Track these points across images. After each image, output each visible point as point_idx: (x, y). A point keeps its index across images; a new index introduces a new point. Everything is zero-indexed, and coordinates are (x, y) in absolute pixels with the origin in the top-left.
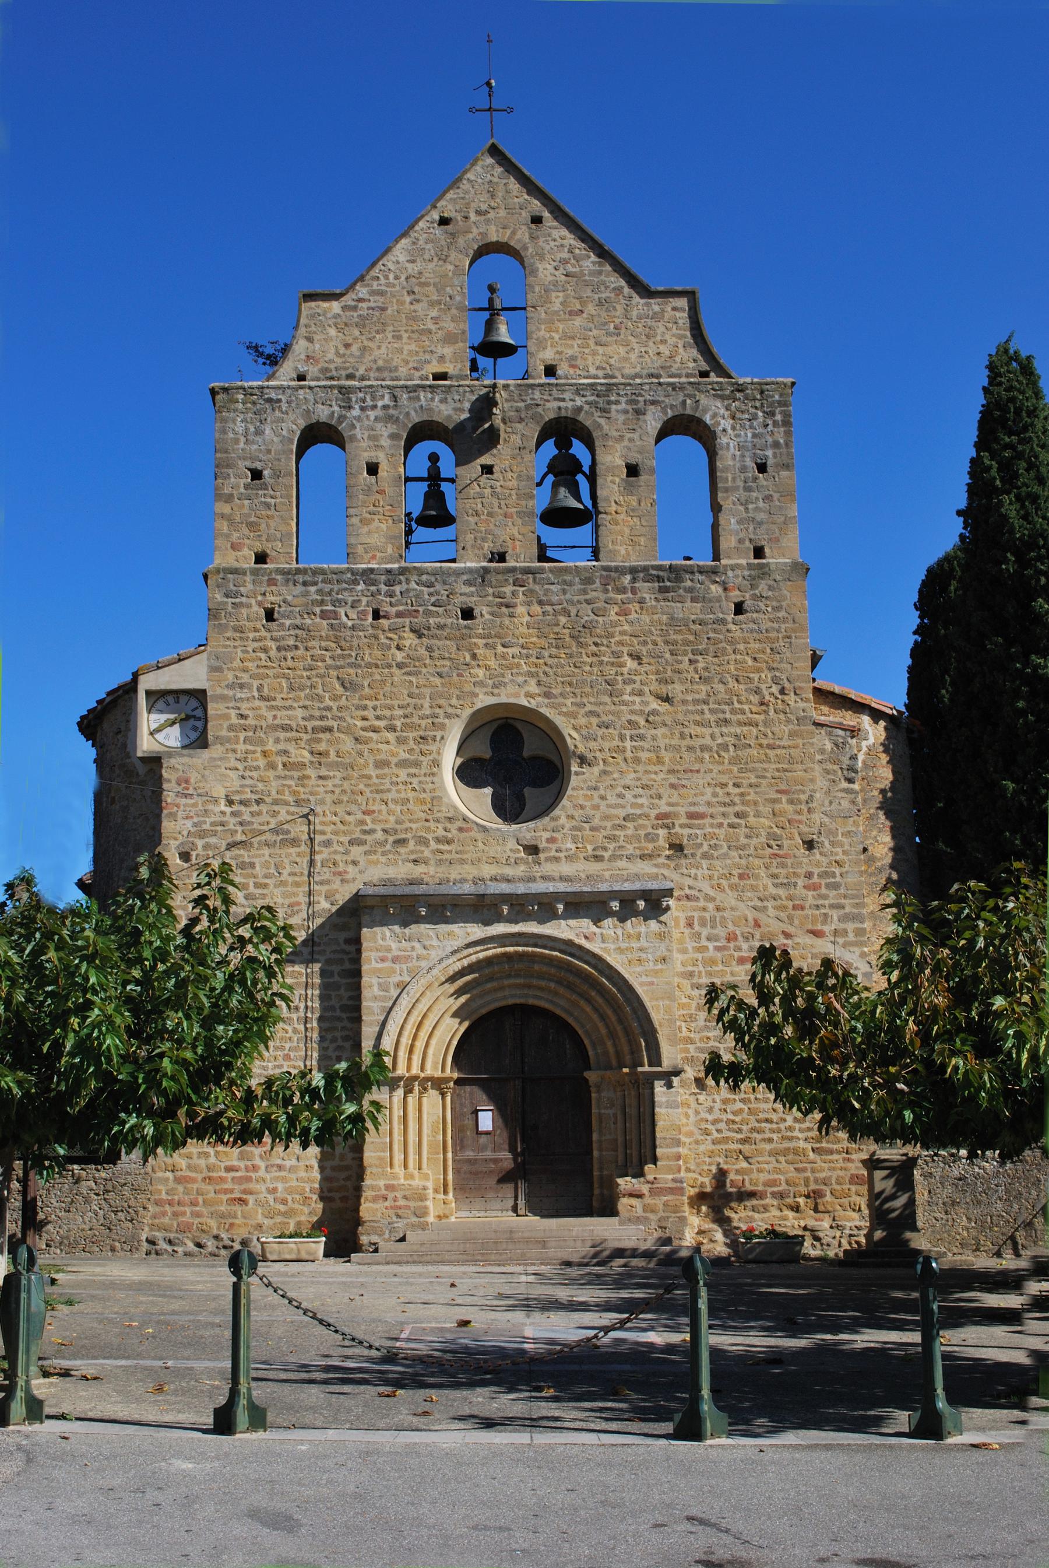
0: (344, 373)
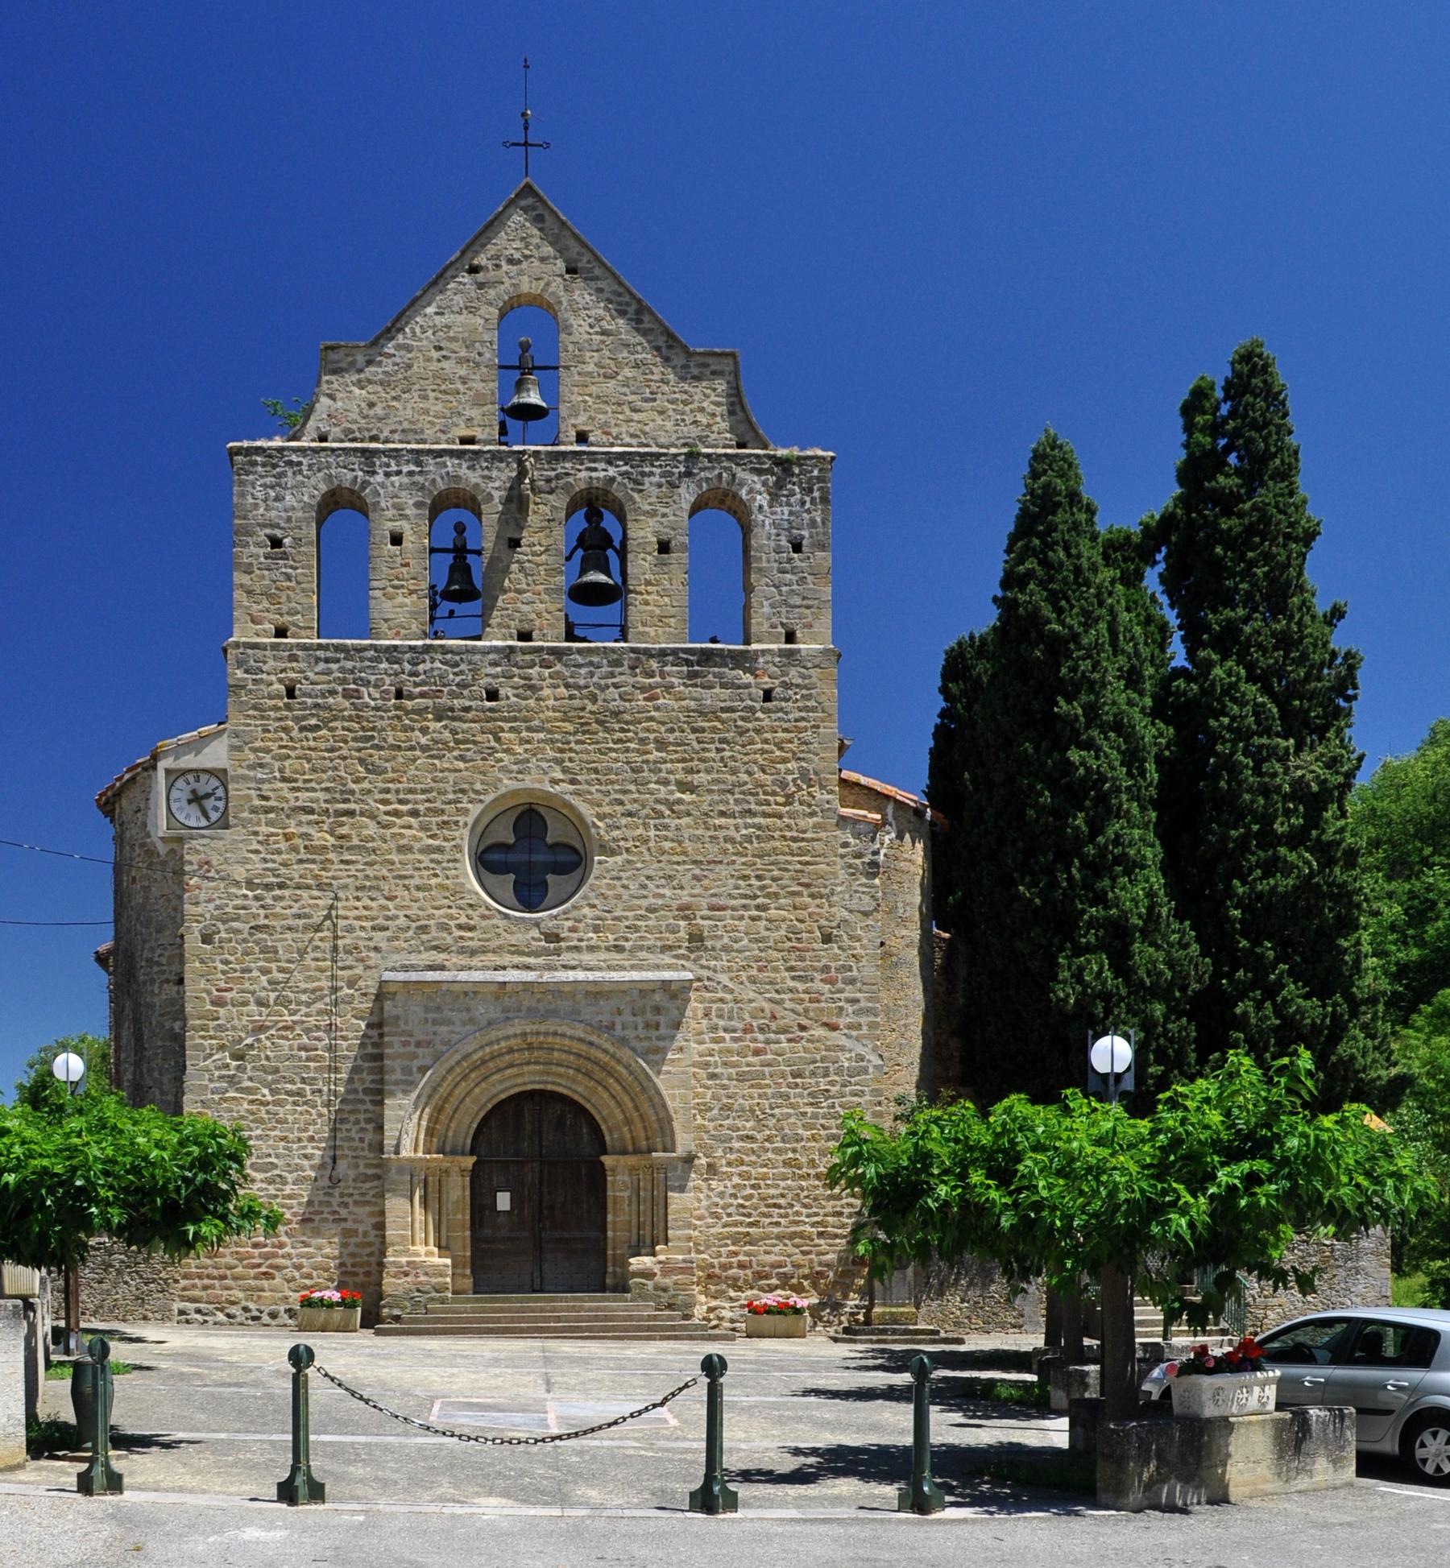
0: (367, 435)
